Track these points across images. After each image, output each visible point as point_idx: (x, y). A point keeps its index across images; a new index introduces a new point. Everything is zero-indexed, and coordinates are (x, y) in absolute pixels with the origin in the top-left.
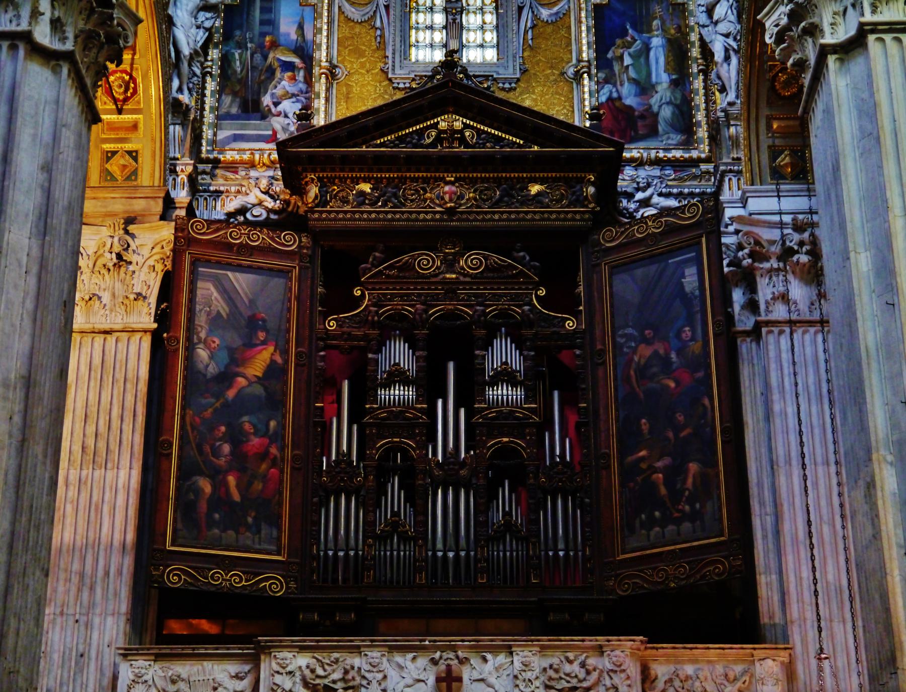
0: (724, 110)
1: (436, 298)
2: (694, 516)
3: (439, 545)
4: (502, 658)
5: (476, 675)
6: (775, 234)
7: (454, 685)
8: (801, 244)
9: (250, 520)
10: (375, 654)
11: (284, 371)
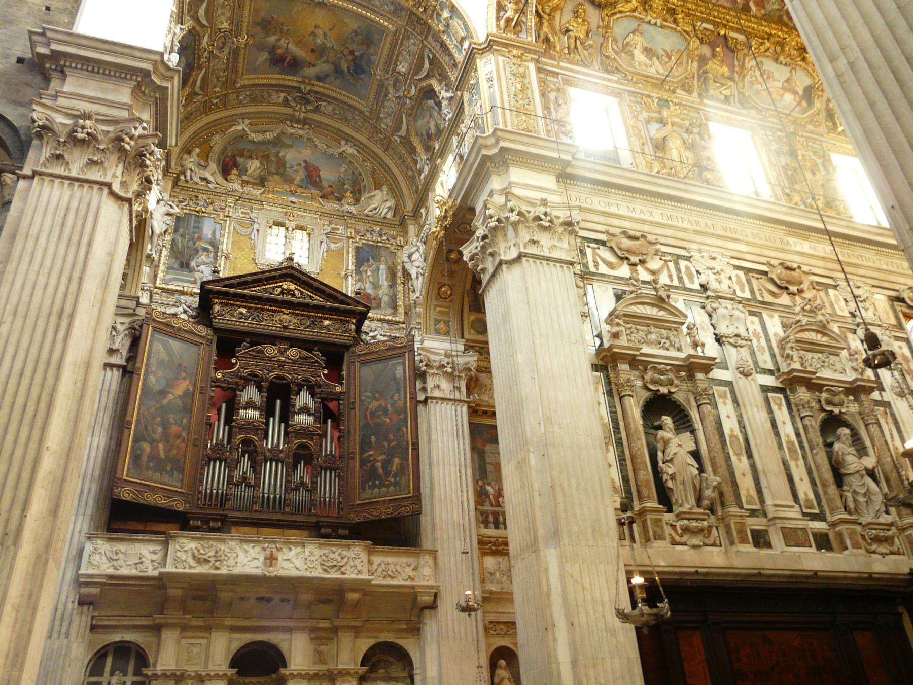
0: (415, 301)
1: (274, 368)
2: (396, 484)
3: (266, 491)
4: (299, 549)
5: (285, 557)
6: (437, 358)
7: (274, 562)
8: (448, 364)
9: (168, 469)
10: (233, 543)
11: (193, 395)
